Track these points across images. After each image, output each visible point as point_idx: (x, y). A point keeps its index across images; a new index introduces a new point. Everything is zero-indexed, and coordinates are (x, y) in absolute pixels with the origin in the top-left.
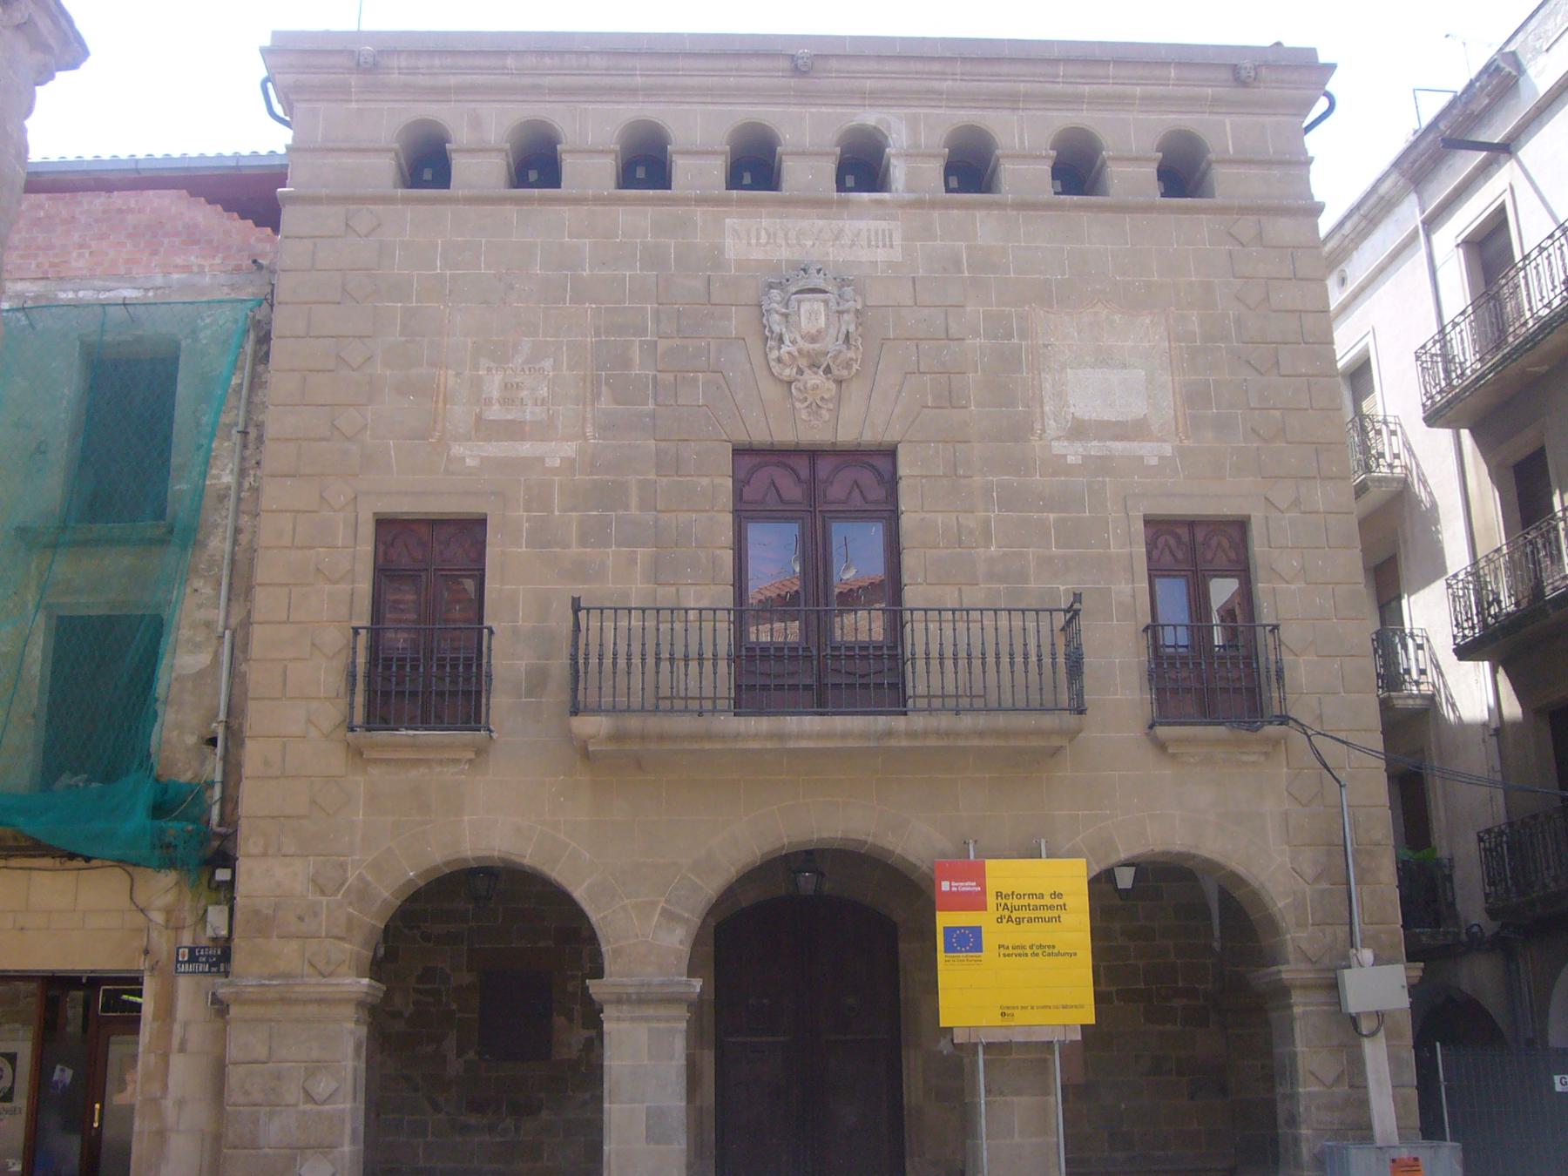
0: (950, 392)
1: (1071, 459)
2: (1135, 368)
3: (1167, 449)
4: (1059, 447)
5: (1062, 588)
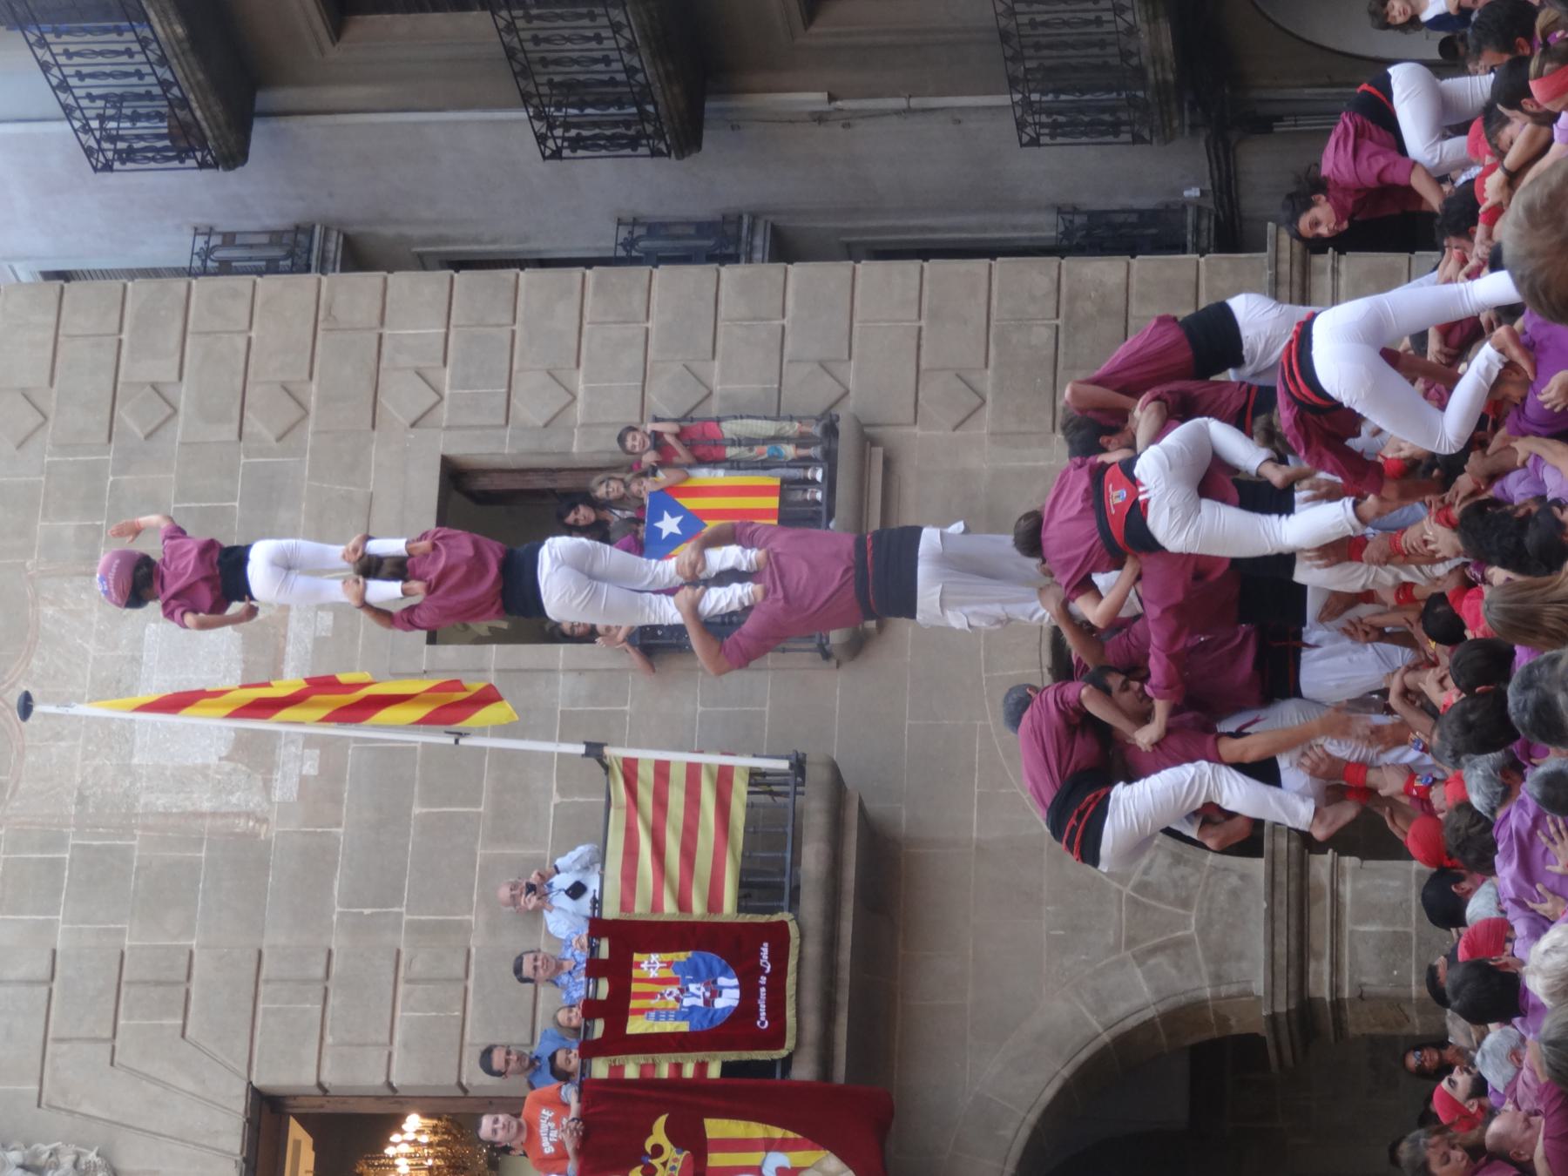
0: (158, 983)
1: (310, 768)
2: (140, 640)
4: (285, 788)
5: (556, 798)
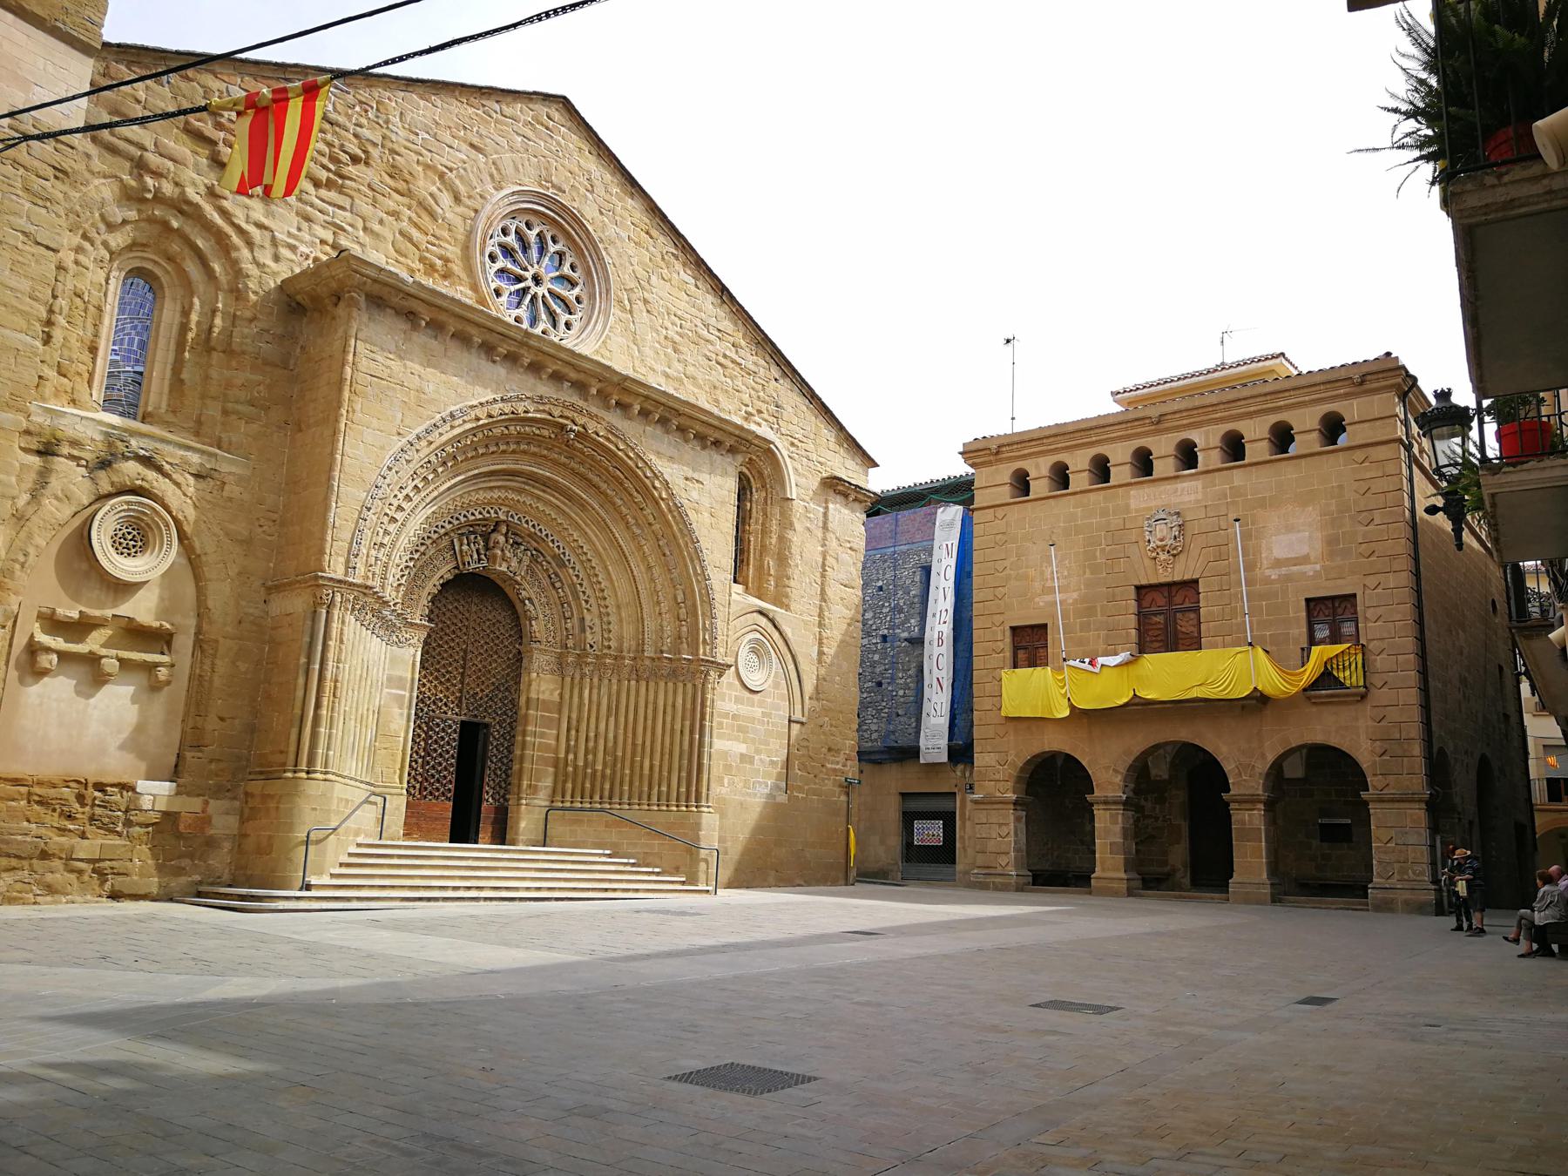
1: (1273, 577)
3: (1318, 567)
4: (1268, 572)
